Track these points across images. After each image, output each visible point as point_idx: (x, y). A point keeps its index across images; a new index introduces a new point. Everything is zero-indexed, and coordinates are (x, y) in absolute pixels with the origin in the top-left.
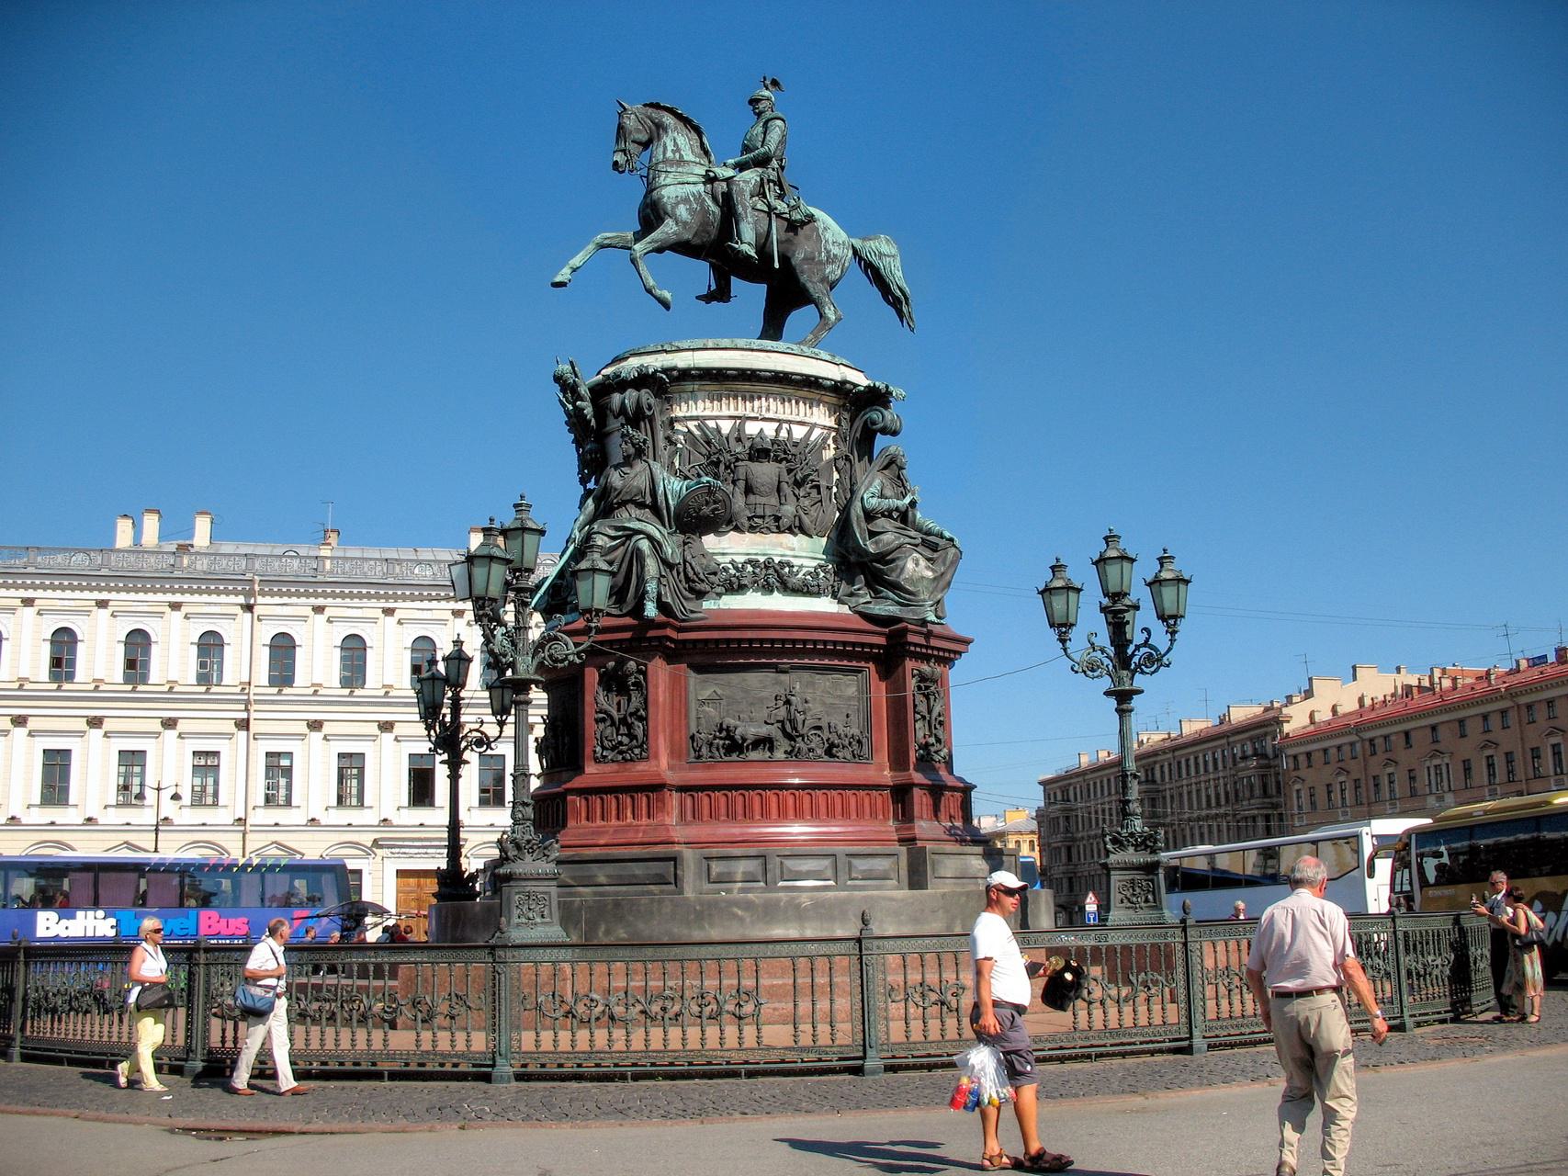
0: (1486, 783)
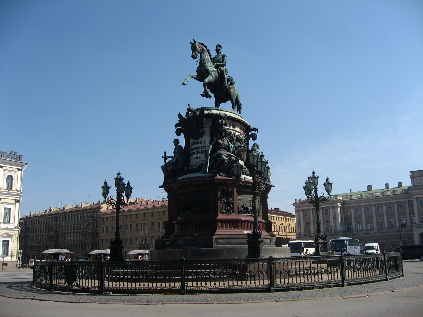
0: (157, 228)
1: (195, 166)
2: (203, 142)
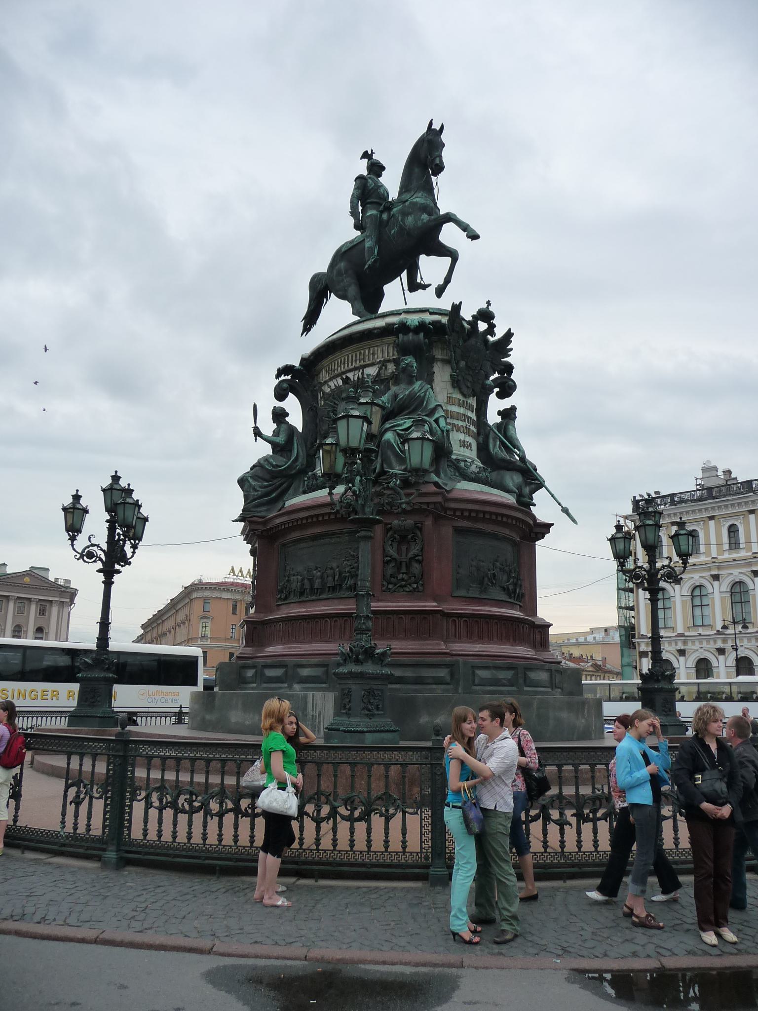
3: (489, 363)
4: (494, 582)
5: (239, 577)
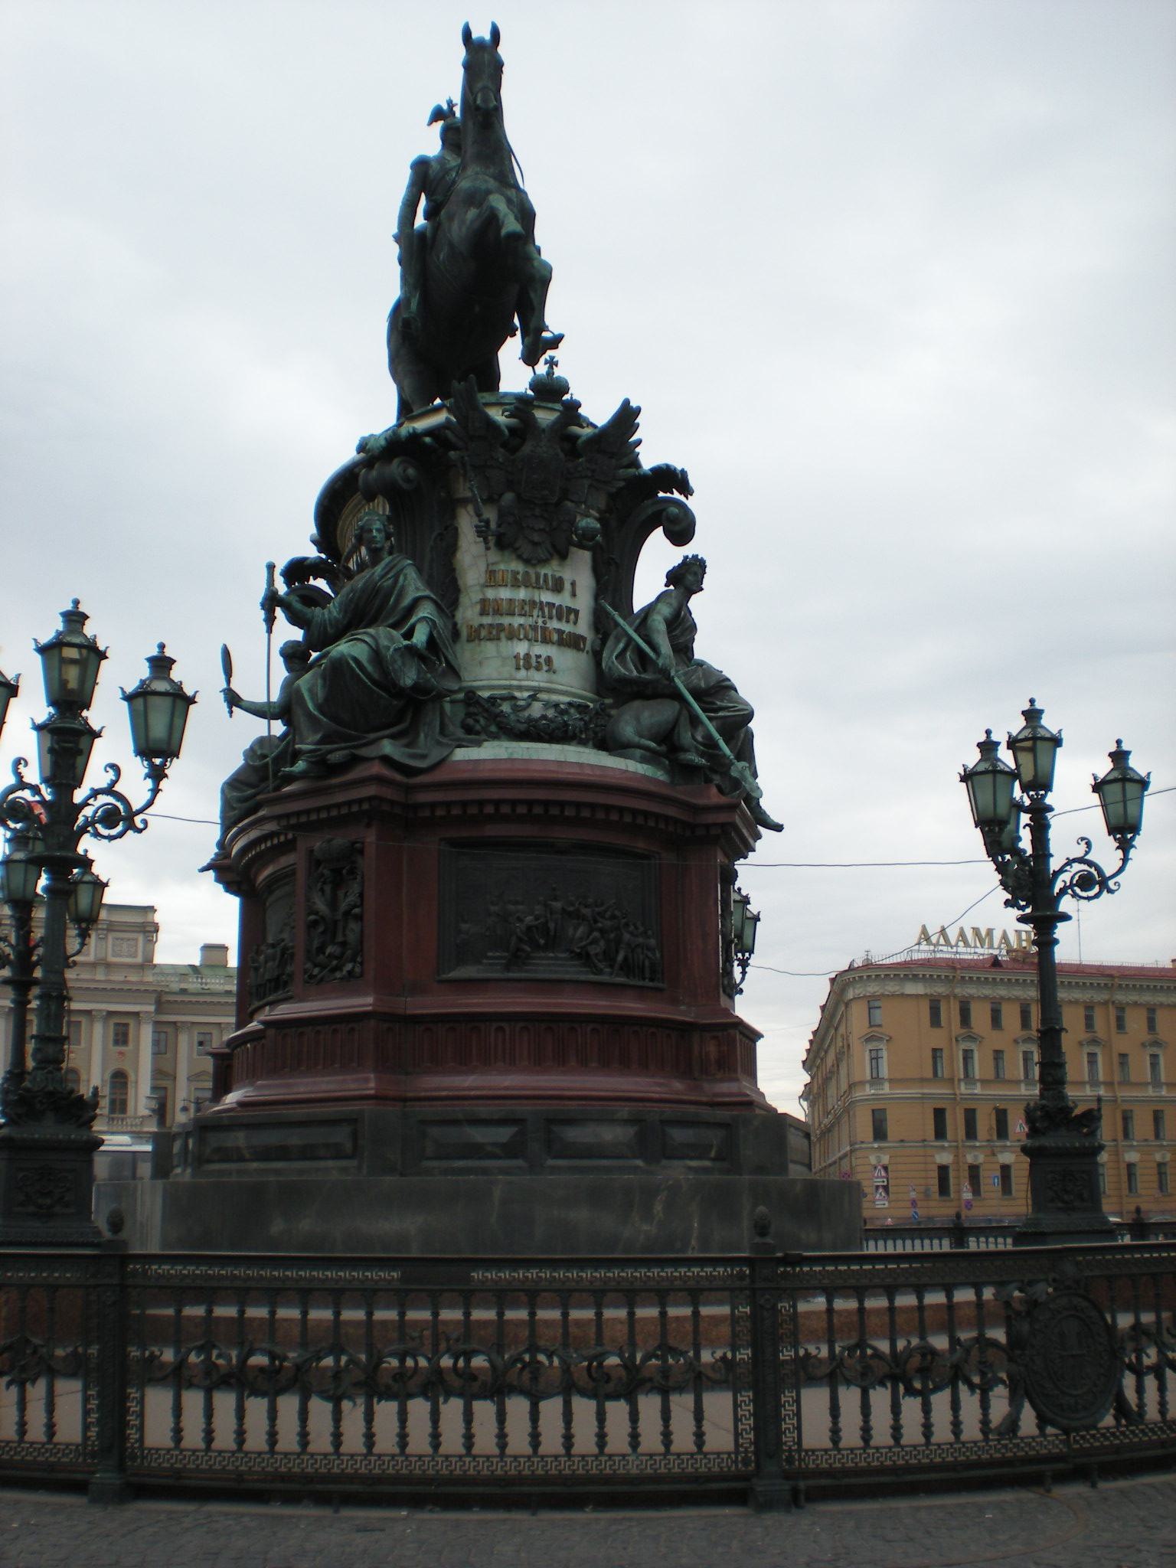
1: (547, 705)
2: (567, 586)
3: (587, 482)
4: (542, 942)
5: (940, 948)
